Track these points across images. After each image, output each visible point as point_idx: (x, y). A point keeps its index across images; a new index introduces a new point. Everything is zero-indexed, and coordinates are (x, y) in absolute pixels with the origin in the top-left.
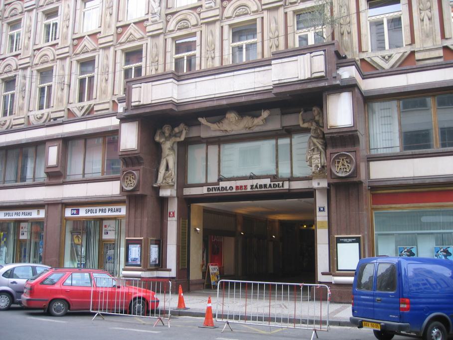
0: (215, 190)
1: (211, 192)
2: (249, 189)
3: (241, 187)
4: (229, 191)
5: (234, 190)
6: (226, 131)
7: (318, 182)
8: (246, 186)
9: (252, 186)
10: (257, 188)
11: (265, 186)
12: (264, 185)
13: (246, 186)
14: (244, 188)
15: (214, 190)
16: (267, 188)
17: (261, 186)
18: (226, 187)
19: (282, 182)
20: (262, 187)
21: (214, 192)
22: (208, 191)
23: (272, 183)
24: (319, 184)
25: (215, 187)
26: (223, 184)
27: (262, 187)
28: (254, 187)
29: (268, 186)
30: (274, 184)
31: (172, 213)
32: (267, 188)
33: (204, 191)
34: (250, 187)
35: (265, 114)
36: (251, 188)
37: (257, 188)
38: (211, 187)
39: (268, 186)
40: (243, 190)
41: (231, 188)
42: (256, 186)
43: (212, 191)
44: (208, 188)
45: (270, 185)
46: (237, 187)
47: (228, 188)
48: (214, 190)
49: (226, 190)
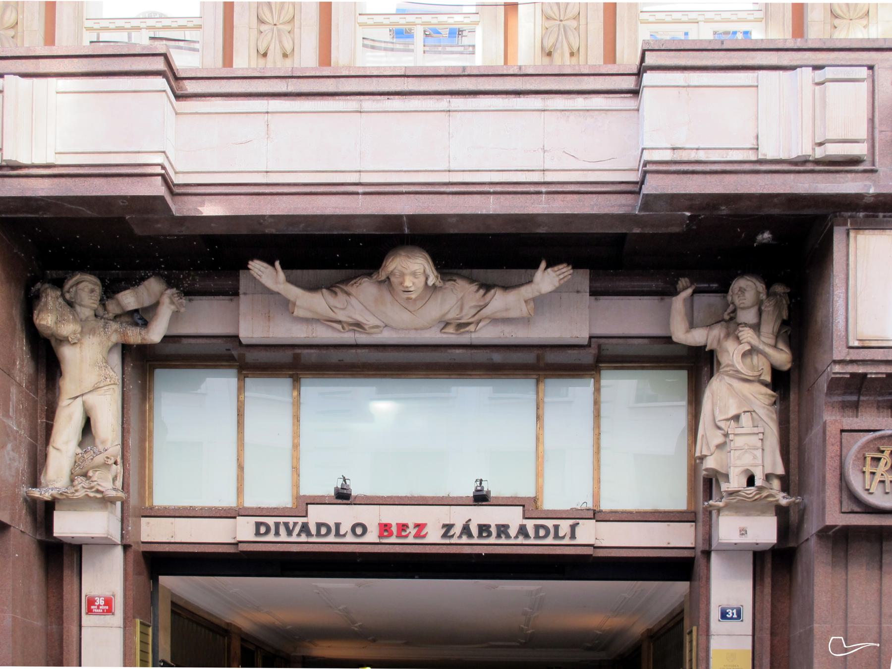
0: (289, 532)
1: (271, 537)
3: (403, 527)
4: (350, 538)
10: (470, 535)
11: (503, 530)
12: (498, 527)
13: (420, 527)
15: (282, 530)
16: (508, 536)
17: (484, 529)
18: (338, 526)
20: (489, 535)
21: (283, 537)
22: (258, 533)
23: (530, 524)
28: (457, 530)
29: (513, 532)
30: (537, 528)
36: (445, 535)
37: (470, 535)
38: (270, 521)
39: (513, 532)
40: (410, 540)
42: (466, 530)
43: (277, 533)
44: (258, 525)
45: (523, 531)
46: (385, 528)
47: (345, 528)
48: (282, 530)
49: (338, 534)
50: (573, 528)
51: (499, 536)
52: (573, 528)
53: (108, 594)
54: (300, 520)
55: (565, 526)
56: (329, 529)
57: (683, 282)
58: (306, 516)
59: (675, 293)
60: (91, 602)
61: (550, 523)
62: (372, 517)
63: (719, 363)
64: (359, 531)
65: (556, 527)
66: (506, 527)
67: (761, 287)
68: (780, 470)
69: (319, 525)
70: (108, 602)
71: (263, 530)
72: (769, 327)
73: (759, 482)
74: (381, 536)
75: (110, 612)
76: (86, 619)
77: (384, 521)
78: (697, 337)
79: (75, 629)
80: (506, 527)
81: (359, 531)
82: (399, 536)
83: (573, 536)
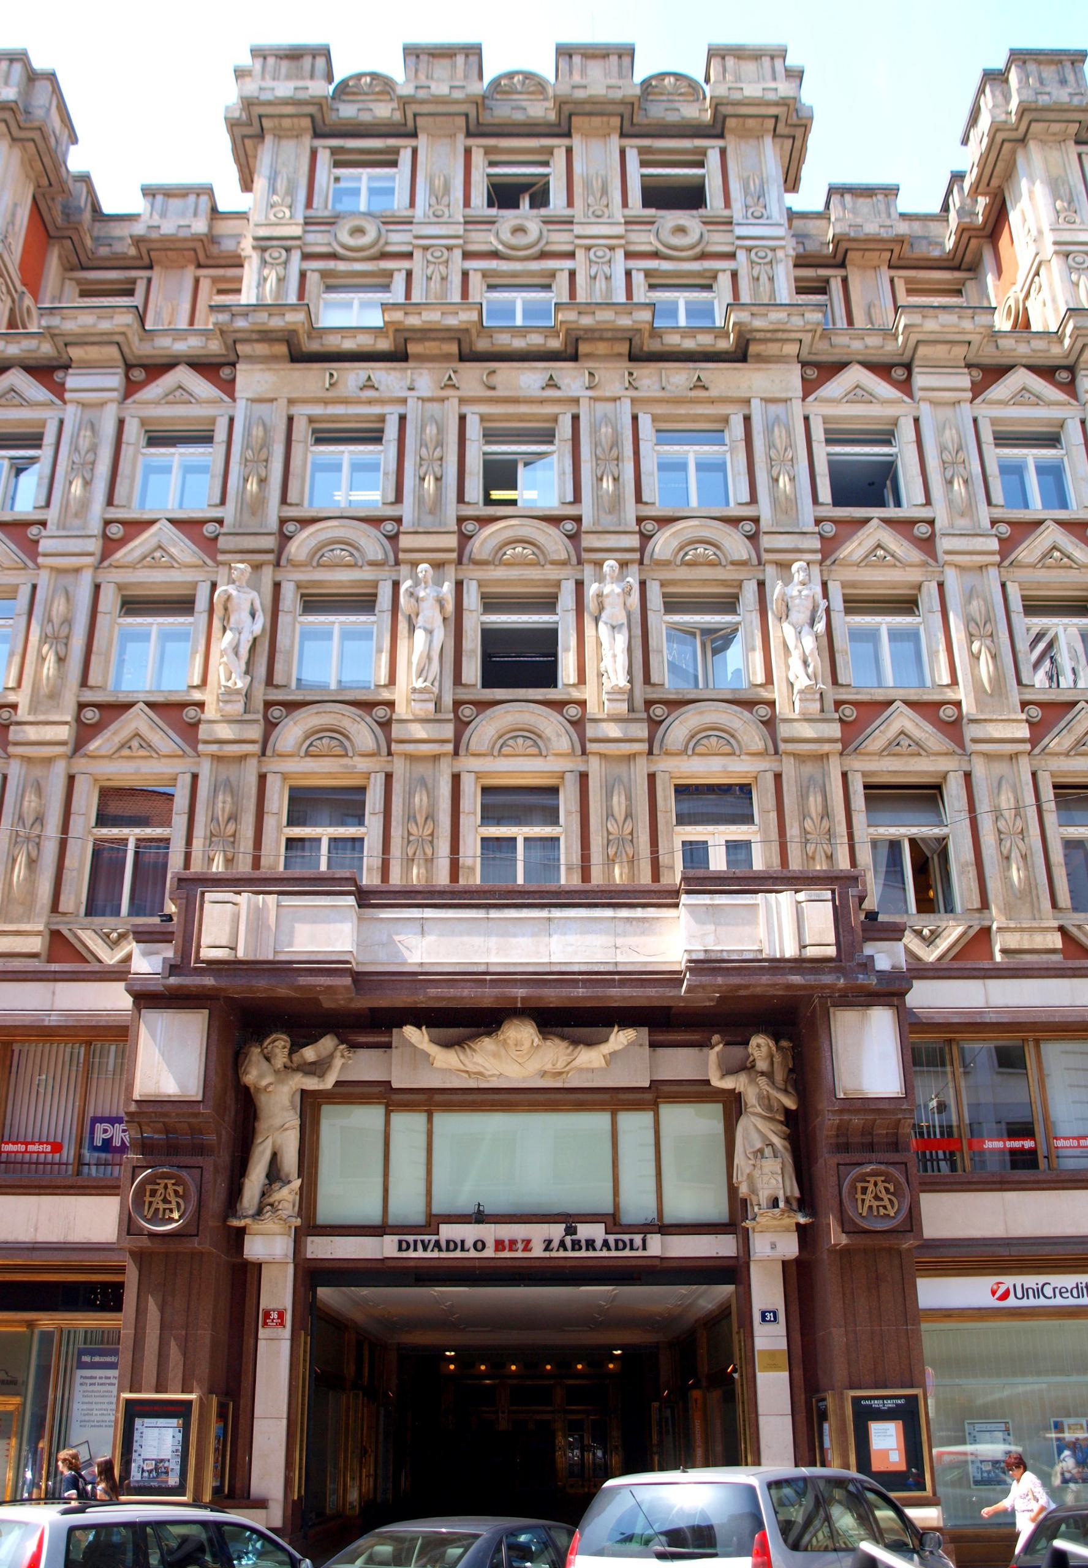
0: (425, 1249)
2: (538, 1251)
3: (513, 1243)
4: (473, 1254)
5: (489, 1253)
6: (480, 1074)
7: (773, 1240)
8: (527, 1243)
9: (548, 1243)
12: (587, 1241)
13: (527, 1243)
14: (520, 1246)
15: (420, 1246)
18: (463, 1242)
19: (642, 1236)
22: (400, 1249)
23: (611, 1238)
24: (773, 1246)
25: (426, 1238)
26: (447, 1232)
27: (580, 1249)
28: (555, 1244)
30: (616, 1241)
31: (274, 1315)
32: (594, 1249)
33: (387, 1247)
34: (543, 1246)
35: (620, 1038)
36: (546, 1249)
38: (410, 1238)
39: (599, 1244)
41: (480, 1245)
43: (415, 1250)
44: (400, 1242)
45: (606, 1243)
46: (499, 1245)
47: (469, 1244)
48: (420, 1246)
50: (644, 1241)
51: (587, 1249)
52: (644, 1241)
53: (281, 1307)
54: (434, 1238)
55: (638, 1239)
56: (455, 1244)
57: (716, 1038)
58: (438, 1234)
59: (712, 1047)
60: (267, 1314)
61: (626, 1238)
62: (489, 1232)
63: (746, 1104)
64: (479, 1246)
65: (631, 1241)
66: (594, 1241)
67: (772, 1044)
68: (797, 1194)
69: (448, 1242)
70: (281, 1315)
71: (404, 1246)
72: (779, 1077)
73: (782, 1204)
74: (497, 1250)
75: (282, 1324)
76: (263, 1333)
77: (499, 1238)
78: (728, 1084)
79: (252, 1342)
80: (594, 1241)
81: (479, 1246)
82: (511, 1250)
83: (644, 1248)
